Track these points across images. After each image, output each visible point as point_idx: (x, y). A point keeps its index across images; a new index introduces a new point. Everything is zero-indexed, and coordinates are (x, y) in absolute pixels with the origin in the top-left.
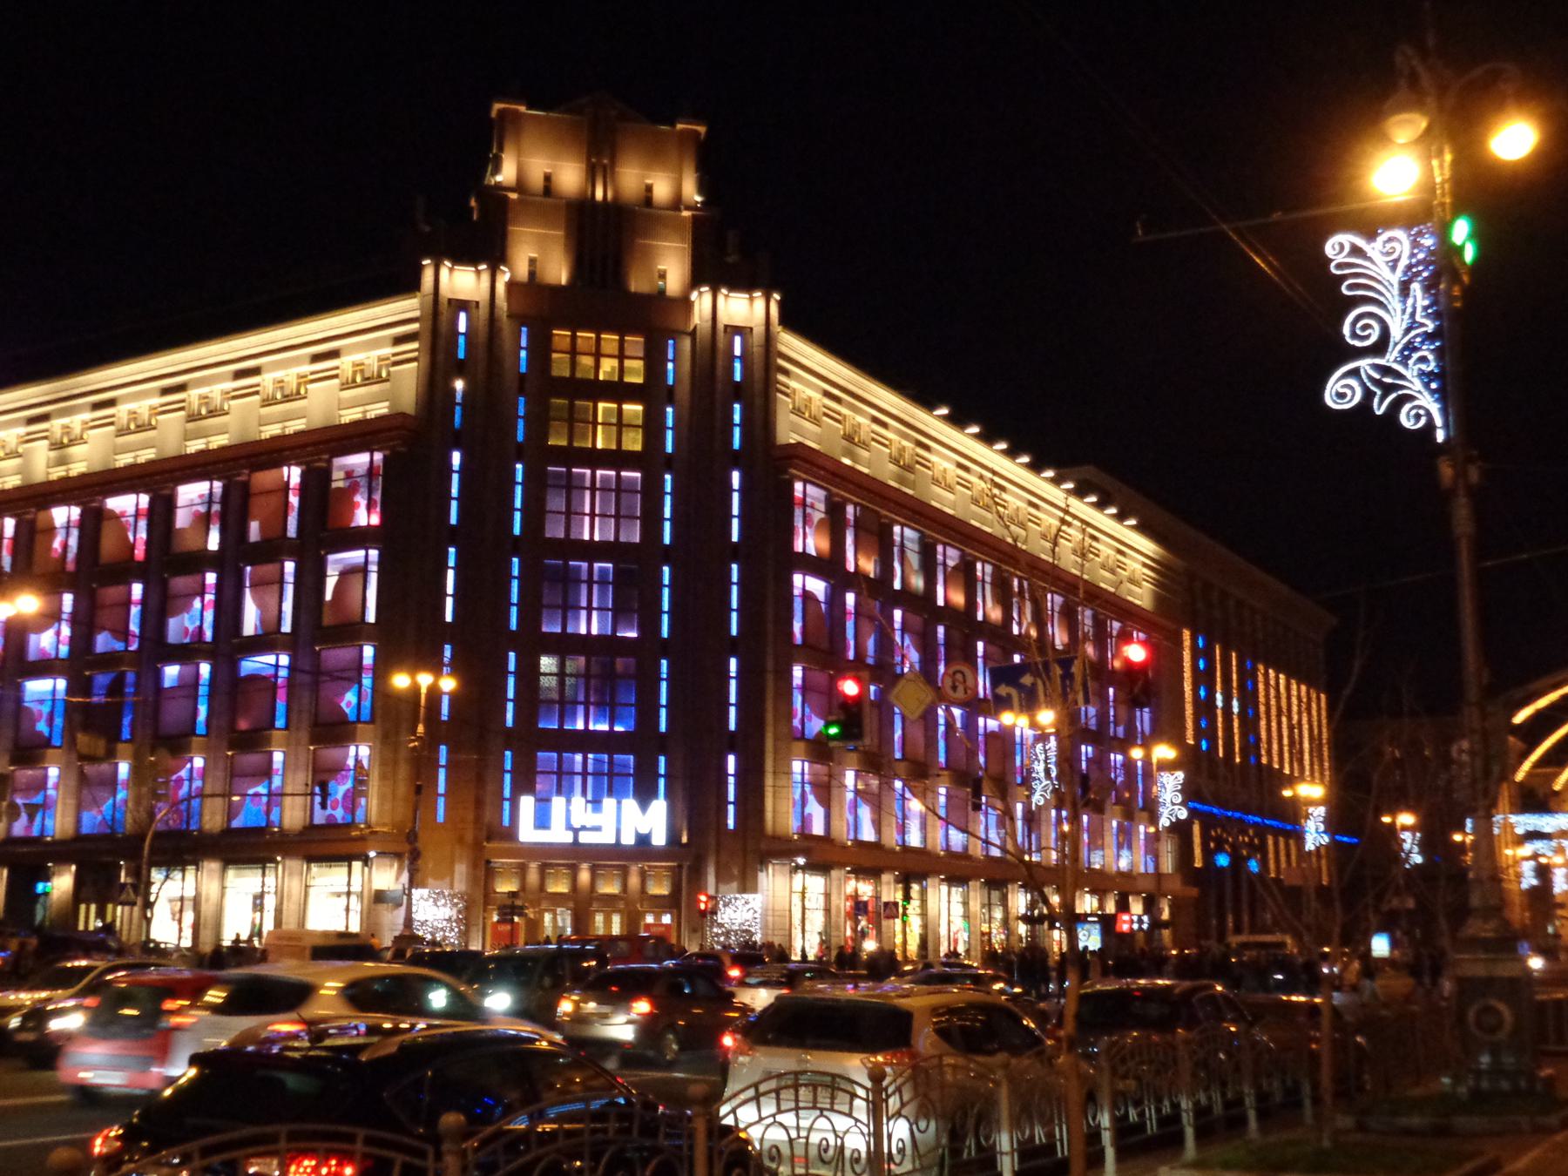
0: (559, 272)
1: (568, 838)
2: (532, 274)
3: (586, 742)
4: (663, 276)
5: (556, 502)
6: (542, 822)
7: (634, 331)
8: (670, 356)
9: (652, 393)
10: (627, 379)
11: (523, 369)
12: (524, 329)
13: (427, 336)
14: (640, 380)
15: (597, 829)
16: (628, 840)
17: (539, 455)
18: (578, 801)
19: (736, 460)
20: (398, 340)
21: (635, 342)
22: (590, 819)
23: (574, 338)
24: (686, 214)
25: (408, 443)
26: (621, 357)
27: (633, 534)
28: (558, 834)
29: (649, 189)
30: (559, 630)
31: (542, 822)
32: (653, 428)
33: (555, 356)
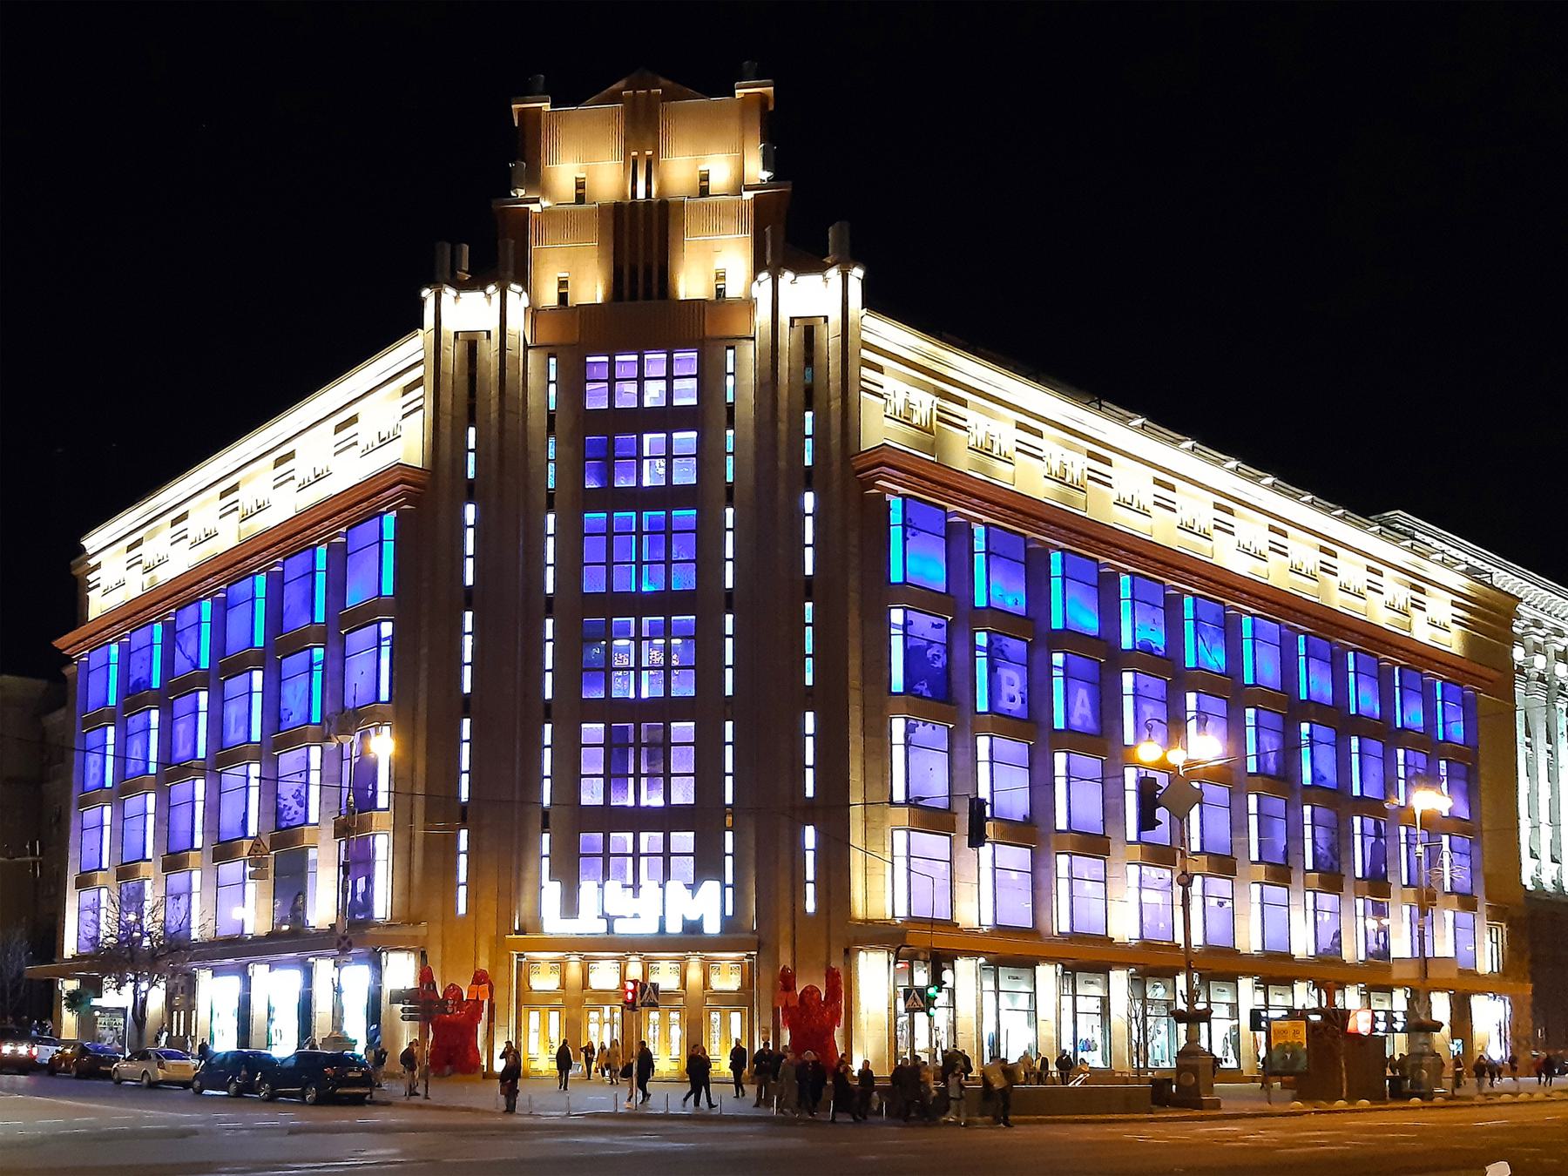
0: (592, 289)
2: (563, 298)
3: (638, 820)
5: (593, 549)
6: (570, 906)
7: (685, 346)
12: (553, 361)
13: (429, 381)
14: (694, 402)
16: (674, 927)
19: (808, 479)
20: (407, 390)
21: (687, 360)
23: (612, 364)
24: (749, 195)
25: (416, 502)
28: (588, 923)
29: (705, 178)
31: (570, 906)
32: (707, 457)
33: (589, 387)
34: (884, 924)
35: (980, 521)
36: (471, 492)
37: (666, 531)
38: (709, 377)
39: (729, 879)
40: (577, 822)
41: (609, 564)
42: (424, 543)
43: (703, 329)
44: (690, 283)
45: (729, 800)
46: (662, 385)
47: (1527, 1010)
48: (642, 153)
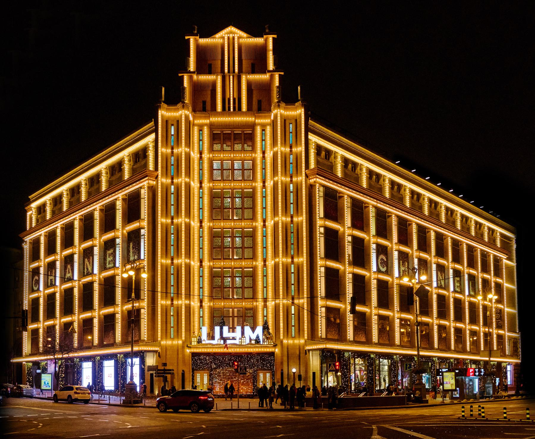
15: (234, 339)
18: (225, 329)
22: (231, 335)
31: (211, 337)
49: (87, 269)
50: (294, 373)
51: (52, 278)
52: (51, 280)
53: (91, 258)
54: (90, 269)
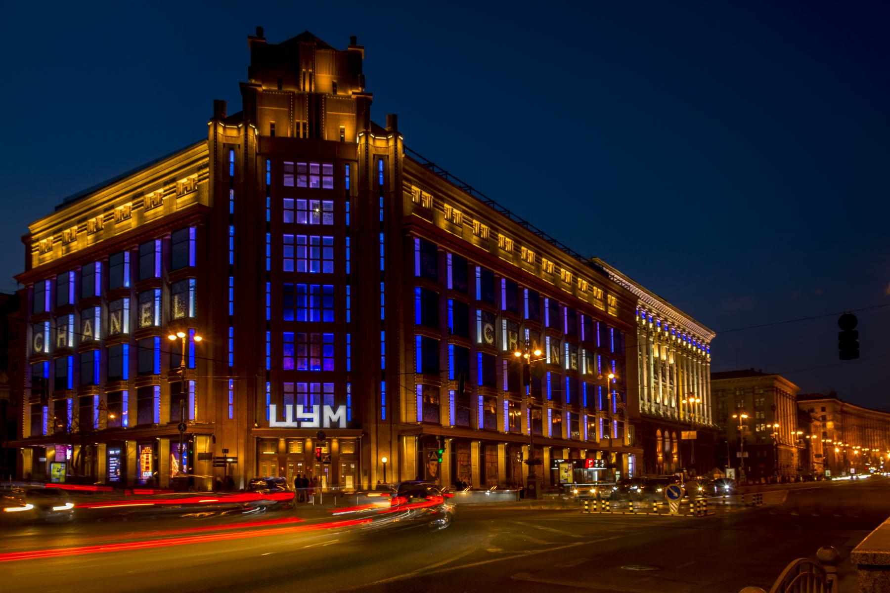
1: (295, 425)
2: (273, 132)
4: (343, 131)
5: (288, 251)
6: (281, 417)
8: (347, 174)
9: (338, 194)
10: (325, 187)
11: (268, 182)
14: (331, 187)
15: (311, 420)
17: (278, 227)
18: (300, 408)
22: (308, 416)
26: (321, 175)
27: (329, 268)
28: (289, 423)
30: (292, 320)
31: (281, 417)
32: (338, 213)
33: (285, 175)
34: (414, 425)
35: (450, 252)
36: (232, 220)
37: (321, 245)
38: (339, 176)
39: (349, 404)
40: (280, 377)
41: (295, 259)
42: (211, 242)
43: (336, 153)
44: (329, 135)
45: (349, 369)
46: (318, 178)
47: (642, 460)
48: (307, 70)
49: (114, 327)
50: (384, 464)
51: (63, 336)
52: (62, 339)
53: (120, 313)
54: (118, 327)
